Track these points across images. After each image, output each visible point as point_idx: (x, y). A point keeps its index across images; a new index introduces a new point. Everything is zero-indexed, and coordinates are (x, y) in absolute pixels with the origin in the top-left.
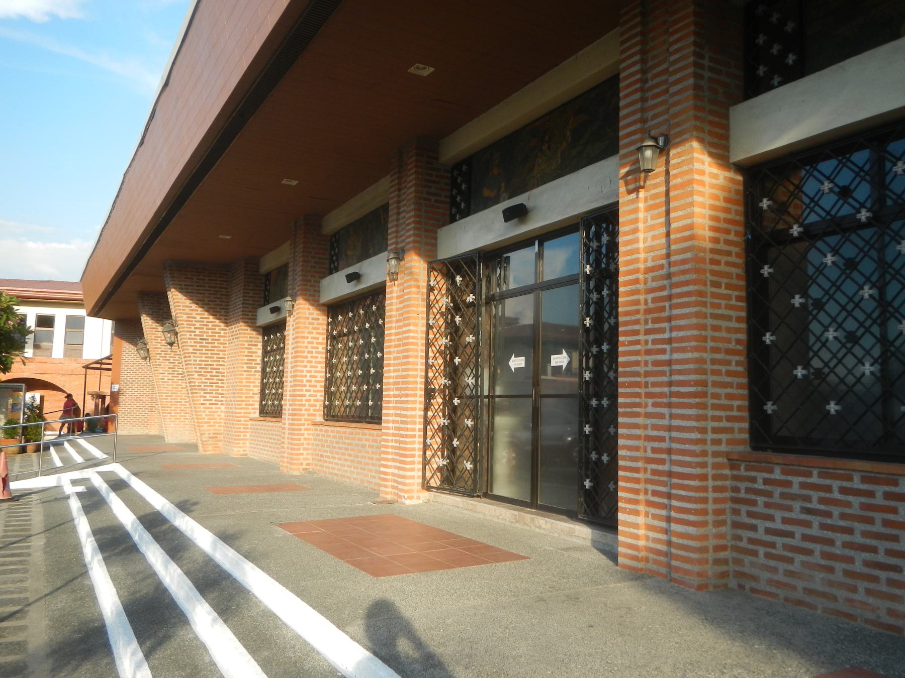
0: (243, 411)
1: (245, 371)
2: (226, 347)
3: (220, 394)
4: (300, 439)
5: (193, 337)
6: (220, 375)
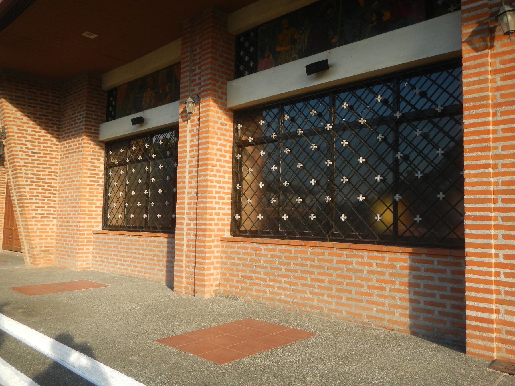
0: (85, 224)
1: (88, 185)
2: (57, 162)
3: (52, 207)
4: (210, 258)
5: (24, 149)
6: (52, 189)
